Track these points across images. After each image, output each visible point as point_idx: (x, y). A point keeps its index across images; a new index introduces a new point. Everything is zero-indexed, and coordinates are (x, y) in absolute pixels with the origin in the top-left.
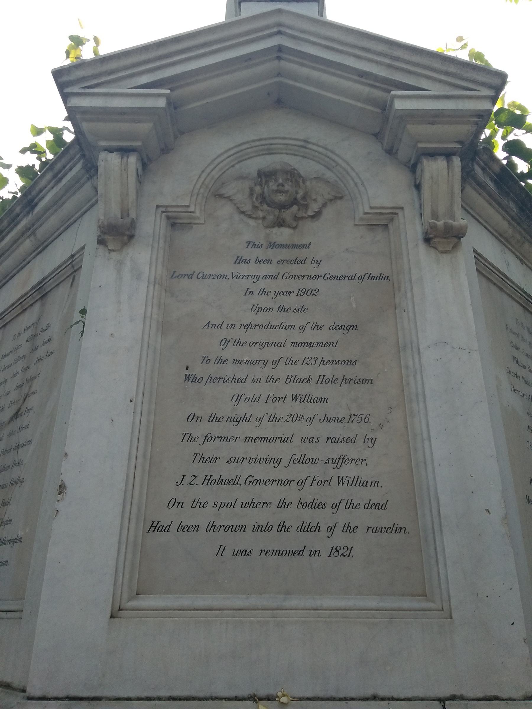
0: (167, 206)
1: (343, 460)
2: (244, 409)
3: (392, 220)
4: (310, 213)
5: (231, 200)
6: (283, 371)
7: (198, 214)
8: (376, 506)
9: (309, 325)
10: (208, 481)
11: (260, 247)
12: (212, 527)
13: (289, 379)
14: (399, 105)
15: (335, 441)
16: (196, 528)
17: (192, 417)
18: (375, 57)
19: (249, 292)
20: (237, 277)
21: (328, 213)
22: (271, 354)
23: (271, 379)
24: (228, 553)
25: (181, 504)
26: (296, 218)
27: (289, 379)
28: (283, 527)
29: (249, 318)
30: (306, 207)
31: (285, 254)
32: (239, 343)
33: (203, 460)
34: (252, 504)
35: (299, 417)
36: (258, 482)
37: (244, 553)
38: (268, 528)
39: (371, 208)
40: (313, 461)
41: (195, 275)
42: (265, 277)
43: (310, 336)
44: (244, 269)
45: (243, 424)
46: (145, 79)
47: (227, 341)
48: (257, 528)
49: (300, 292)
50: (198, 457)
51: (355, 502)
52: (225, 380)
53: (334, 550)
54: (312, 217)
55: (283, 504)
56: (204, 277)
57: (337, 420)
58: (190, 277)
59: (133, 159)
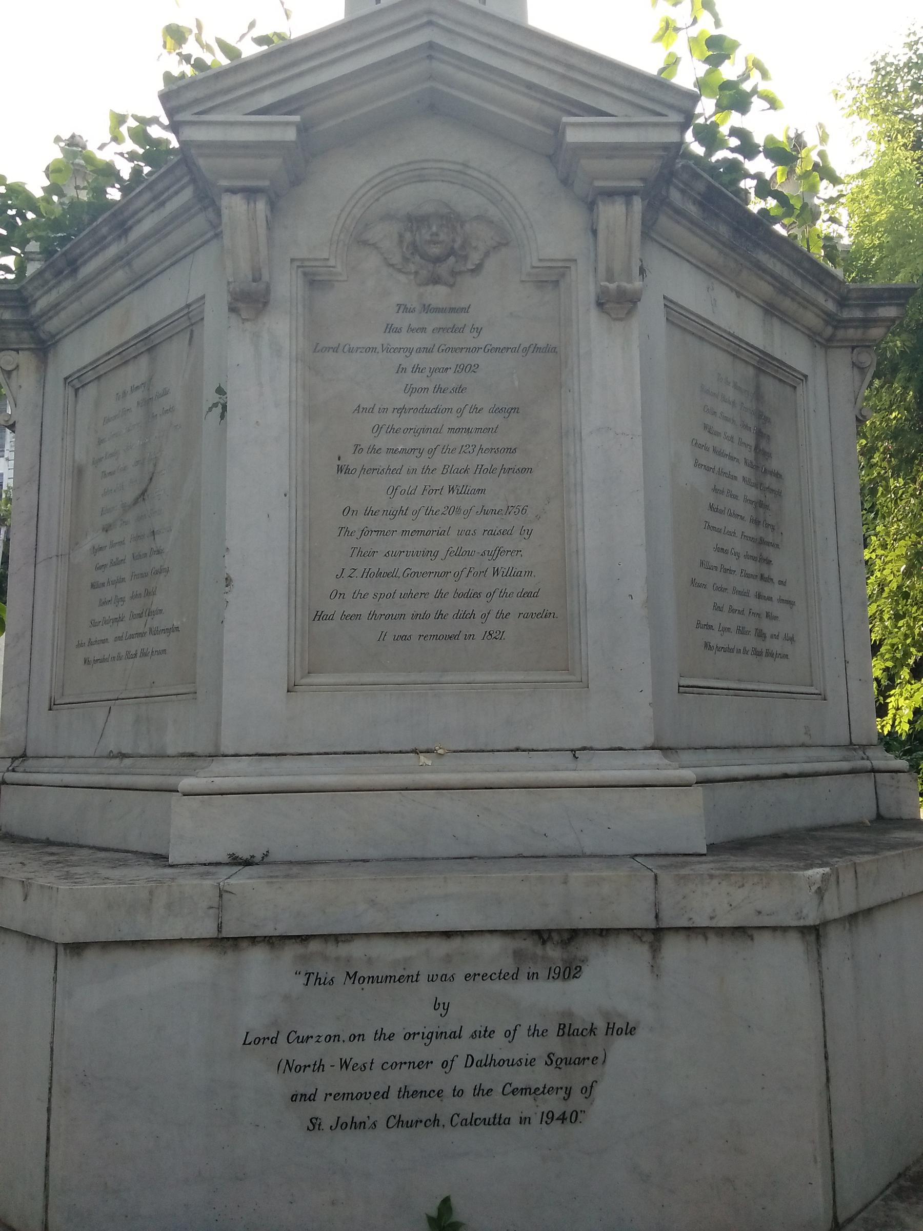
0: (303, 260)
1: (500, 551)
2: (399, 501)
3: (563, 275)
4: (470, 266)
5: (377, 248)
6: (439, 461)
7: (339, 269)
8: (529, 594)
9: (468, 408)
10: (367, 574)
11: (412, 311)
12: (373, 616)
13: (447, 470)
14: (573, 136)
15: (492, 533)
16: (358, 616)
17: (347, 511)
18: (547, 65)
20: (388, 350)
21: (491, 265)
22: (427, 441)
23: (427, 470)
24: (389, 638)
25: (342, 595)
26: (454, 273)
27: (447, 470)
28: (440, 615)
29: (402, 400)
30: (466, 258)
31: (440, 320)
32: (392, 430)
33: (361, 554)
34: (411, 595)
35: (457, 510)
36: (416, 574)
37: (404, 638)
38: (425, 616)
39: (540, 260)
40: (469, 554)
41: (341, 348)
42: (419, 350)
43: (469, 420)
44: (396, 340)
45: (400, 517)
46: (268, 99)
47: (380, 428)
48: (415, 616)
49: (458, 369)
50: (356, 551)
51: (509, 591)
53: (488, 634)
54: (472, 271)
55: (440, 595)
56: (351, 351)
57: (494, 512)
58: (335, 350)
59: (261, 206)
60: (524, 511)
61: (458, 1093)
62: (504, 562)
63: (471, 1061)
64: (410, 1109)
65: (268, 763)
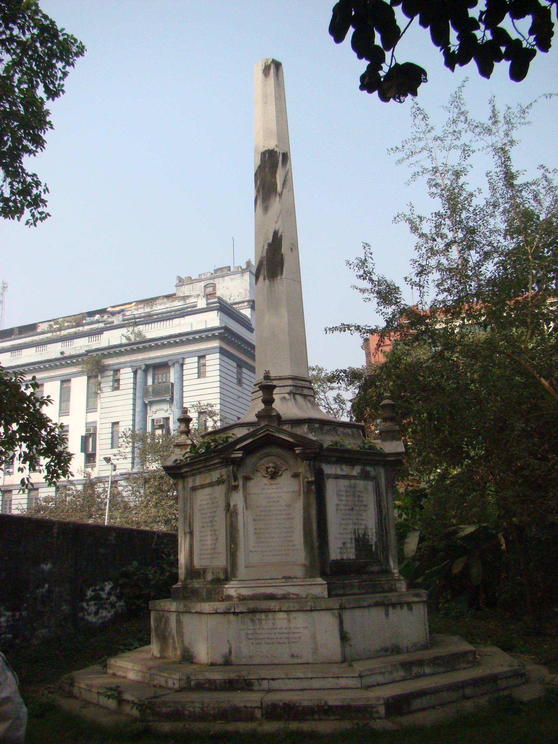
10: (260, 542)
19: (266, 498)
52: (262, 520)
60: (292, 527)
61: (277, 638)
62: (288, 539)
63: (279, 633)
64: (268, 641)
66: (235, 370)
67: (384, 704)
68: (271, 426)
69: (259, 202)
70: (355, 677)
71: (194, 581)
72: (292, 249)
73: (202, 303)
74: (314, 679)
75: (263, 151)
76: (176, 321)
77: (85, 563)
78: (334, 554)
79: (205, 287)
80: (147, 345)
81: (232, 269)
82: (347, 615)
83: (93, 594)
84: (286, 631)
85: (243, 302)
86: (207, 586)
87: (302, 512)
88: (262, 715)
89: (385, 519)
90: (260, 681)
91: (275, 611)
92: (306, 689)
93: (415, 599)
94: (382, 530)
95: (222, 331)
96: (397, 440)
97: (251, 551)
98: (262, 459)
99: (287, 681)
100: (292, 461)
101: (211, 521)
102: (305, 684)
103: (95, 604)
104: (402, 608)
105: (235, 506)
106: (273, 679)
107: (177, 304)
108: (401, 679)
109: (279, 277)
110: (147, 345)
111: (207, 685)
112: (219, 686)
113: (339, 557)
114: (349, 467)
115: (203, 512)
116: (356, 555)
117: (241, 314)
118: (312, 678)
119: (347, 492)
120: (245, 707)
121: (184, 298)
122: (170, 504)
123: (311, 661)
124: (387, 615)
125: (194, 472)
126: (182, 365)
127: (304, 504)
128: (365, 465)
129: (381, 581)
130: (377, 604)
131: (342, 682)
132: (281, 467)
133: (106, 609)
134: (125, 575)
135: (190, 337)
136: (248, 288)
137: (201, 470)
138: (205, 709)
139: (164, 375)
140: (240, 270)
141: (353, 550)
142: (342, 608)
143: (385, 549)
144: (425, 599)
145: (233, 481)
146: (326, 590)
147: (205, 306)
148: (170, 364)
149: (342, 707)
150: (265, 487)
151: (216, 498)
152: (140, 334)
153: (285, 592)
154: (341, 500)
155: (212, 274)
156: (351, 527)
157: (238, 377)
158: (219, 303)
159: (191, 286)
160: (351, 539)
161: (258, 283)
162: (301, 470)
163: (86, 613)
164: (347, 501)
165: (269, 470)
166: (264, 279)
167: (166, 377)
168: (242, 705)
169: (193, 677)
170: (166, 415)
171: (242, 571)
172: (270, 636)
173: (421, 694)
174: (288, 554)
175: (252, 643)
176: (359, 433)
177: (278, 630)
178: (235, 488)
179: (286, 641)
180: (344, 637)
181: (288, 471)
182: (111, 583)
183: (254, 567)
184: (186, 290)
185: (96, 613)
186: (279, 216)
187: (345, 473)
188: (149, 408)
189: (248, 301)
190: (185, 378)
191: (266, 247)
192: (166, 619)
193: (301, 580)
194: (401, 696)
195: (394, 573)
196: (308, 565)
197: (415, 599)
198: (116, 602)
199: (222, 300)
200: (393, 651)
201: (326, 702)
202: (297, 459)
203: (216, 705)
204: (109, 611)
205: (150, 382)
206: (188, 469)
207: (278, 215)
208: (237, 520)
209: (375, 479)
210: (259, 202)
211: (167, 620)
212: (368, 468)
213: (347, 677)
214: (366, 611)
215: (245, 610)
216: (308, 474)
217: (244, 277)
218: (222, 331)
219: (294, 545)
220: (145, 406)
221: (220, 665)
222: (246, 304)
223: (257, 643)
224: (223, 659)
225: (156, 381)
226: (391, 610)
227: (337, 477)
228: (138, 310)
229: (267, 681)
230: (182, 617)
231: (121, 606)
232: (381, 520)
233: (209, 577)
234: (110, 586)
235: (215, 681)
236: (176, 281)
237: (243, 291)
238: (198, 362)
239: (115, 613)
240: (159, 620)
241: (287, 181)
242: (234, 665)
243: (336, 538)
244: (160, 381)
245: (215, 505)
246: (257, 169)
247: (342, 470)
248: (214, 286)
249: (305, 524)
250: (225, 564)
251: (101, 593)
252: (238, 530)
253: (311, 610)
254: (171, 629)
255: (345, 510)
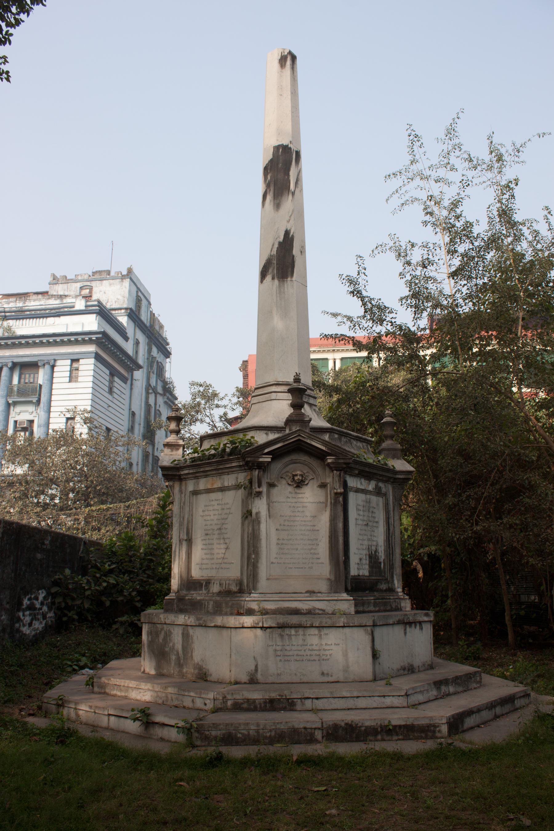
1: (312, 549)
10: (283, 554)
19: (290, 507)
30: (304, 482)
32: (288, 521)
35: (302, 539)
44: (289, 500)
52: (285, 530)
60: (317, 540)
61: (307, 655)
62: (312, 551)
64: (298, 658)
65: (263, 595)
66: (107, 378)
67: (447, 723)
68: (304, 431)
69: (269, 198)
70: (402, 696)
71: (192, 592)
72: (301, 252)
73: (80, 305)
74: (359, 698)
75: (277, 145)
76: (51, 320)
77: (24, 568)
78: (354, 571)
79: (81, 288)
80: (17, 341)
81: (112, 274)
82: (378, 632)
83: (28, 603)
84: (317, 648)
85: (121, 309)
86: (214, 598)
87: (328, 524)
88: (323, 737)
89: (392, 537)
90: (303, 700)
91: (305, 627)
92: (351, 709)
93: (426, 619)
94: (389, 547)
95: (100, 336)
96: (398, 459)
97: (272, 563)
98: (287, 465)
99: (331, 700)
100: (319, 470)
101: (220, 529)
102: (350, 703)
103: (30, 615)
104: (415, 627)
105: (258, 514)
106: (317, 699)
107: (53, 303)
108: (434, 698)
109: (289, 279)
110: (17, 341)
111: (245, 706)
112: (259, 706)
113: (356, 574)
114: (366, 481)
115: (208, 518)
116: (369, 572)
117: (118, 321)
118: (358, 697)
119: (363, 506)
120: (305, 728)
121: (61, 297)
122: (36, 511)
123: (341, 679)
124: (405, 633)
125: (197, 475)
126: (53, 367)
127: (331, 515)
128: (379, 480)
129: (390, 599)
130: (399, 622)
131: (388, 701)
132: (308, 476)
133: (39, 620)
134: (56, 583)
135: (65, 339)
136: (127, 295)
137: (208, 473)
138: (261, 731)
139: (32, 376)
140: (120, 275)
141: (367, 567)
142: (374, 625)
143: (392, 567)
144: (432, 619)
145: (257, 486)
146: (353, 606)
147: (83, 308)
148: (39, 364)
149: (406, 727)
150: (290, 496)
151: (227, 504)
152: (9, 329)
153: (311, 607)
154: (359, 515)
155: (90, 276)
156: (366, 543)
157: (109, 385)
158: (99, 306)
159: (65, 286)
160: (366, 555)
161: (265, 281)
162: (329, 480)
163: (22, 624)
164: (364, 516)
165: (296, 478)
166: (273, 278)
167: (34, 378)
168: (302, 726)
169: (229, 697)
170: (31, 418)
171: (263, 583)
172: (300, 653)
173: (470, 713)
174: (312, 568)
175: (281, 660)
176: (368, 447)
177: (308, 647)
178: (259, 494)
179: (317, 658)
180: (375, 655)
181: (315, 480)
182: (44, 591)
183: (276, 579)
184: (60, 289)
185: (30, 624)
186: (291, 215)
187: (363, 487)
188: (12, 408)
189: (126, 309)
190: (55, 380)
191: (276, 246)
192: (166, 633)
193: (326, 594)
194: (457, 714)
195: (398, 592)
196: (333, 579)
197: (426, 619)
198: (47, 613)
199: (102, 304)
200: (409, 670)
201: (390, 722)
202: (325, 470)
203: (273, 727)
204: (41, 623)
205: (15, 381)
206: (191, 471)
207: (290, 214)
208: (259, 529)
209: (385, 495)
210: (269, 198)
211: (168, 635)
212: (381, 485)
213: (393, 696)
214: (390, 629)
215: (274, 625)
216: (337, 485)
217: (124, 284)
218: (100, 336)
219: (318, 559)
220: (8, 405)
221: (245, 683)
222: (123, 311)
223: (285, 661)
224: (248, 678)
225: (22, 380)
226: (408, 629)
227: (357, 491)
228: (9, 303)
229: (310, 700)
230: (191, 631)
231: (51, 617)
232: (389, 537)
233: (215, 588)
234: (43, 595)
235: (254, 700)
236: (50, 279)
237: (120, 297)
238: (71, 365)
239: (45, 624)
240: (154, 634)
241: (298, 181)
242: (259, 683)
243: (355, 553)
244: (27, 381)
245: (228, 511)
246: (267, 162)
247: (361, 484)
248: (91, 289)
249: (331, 537)
250: (238, 574)
251: (35, 602)
252: (261, 540)
253: (344, 627)
254: (174, 644)
255: (362, 525)
